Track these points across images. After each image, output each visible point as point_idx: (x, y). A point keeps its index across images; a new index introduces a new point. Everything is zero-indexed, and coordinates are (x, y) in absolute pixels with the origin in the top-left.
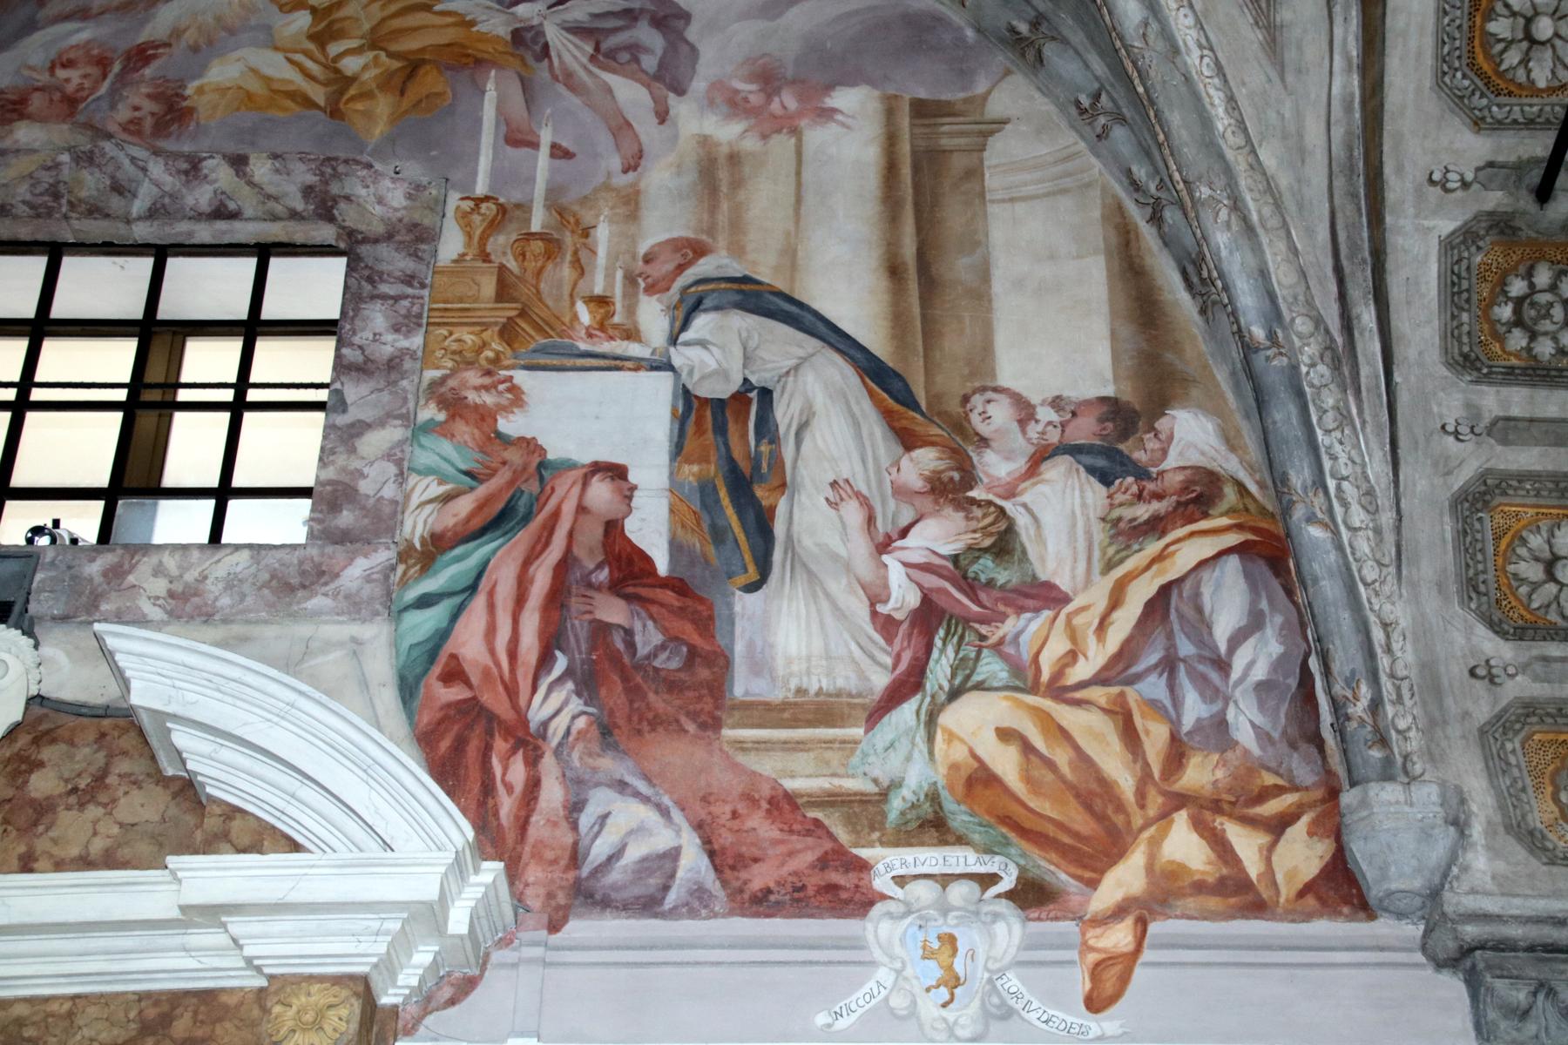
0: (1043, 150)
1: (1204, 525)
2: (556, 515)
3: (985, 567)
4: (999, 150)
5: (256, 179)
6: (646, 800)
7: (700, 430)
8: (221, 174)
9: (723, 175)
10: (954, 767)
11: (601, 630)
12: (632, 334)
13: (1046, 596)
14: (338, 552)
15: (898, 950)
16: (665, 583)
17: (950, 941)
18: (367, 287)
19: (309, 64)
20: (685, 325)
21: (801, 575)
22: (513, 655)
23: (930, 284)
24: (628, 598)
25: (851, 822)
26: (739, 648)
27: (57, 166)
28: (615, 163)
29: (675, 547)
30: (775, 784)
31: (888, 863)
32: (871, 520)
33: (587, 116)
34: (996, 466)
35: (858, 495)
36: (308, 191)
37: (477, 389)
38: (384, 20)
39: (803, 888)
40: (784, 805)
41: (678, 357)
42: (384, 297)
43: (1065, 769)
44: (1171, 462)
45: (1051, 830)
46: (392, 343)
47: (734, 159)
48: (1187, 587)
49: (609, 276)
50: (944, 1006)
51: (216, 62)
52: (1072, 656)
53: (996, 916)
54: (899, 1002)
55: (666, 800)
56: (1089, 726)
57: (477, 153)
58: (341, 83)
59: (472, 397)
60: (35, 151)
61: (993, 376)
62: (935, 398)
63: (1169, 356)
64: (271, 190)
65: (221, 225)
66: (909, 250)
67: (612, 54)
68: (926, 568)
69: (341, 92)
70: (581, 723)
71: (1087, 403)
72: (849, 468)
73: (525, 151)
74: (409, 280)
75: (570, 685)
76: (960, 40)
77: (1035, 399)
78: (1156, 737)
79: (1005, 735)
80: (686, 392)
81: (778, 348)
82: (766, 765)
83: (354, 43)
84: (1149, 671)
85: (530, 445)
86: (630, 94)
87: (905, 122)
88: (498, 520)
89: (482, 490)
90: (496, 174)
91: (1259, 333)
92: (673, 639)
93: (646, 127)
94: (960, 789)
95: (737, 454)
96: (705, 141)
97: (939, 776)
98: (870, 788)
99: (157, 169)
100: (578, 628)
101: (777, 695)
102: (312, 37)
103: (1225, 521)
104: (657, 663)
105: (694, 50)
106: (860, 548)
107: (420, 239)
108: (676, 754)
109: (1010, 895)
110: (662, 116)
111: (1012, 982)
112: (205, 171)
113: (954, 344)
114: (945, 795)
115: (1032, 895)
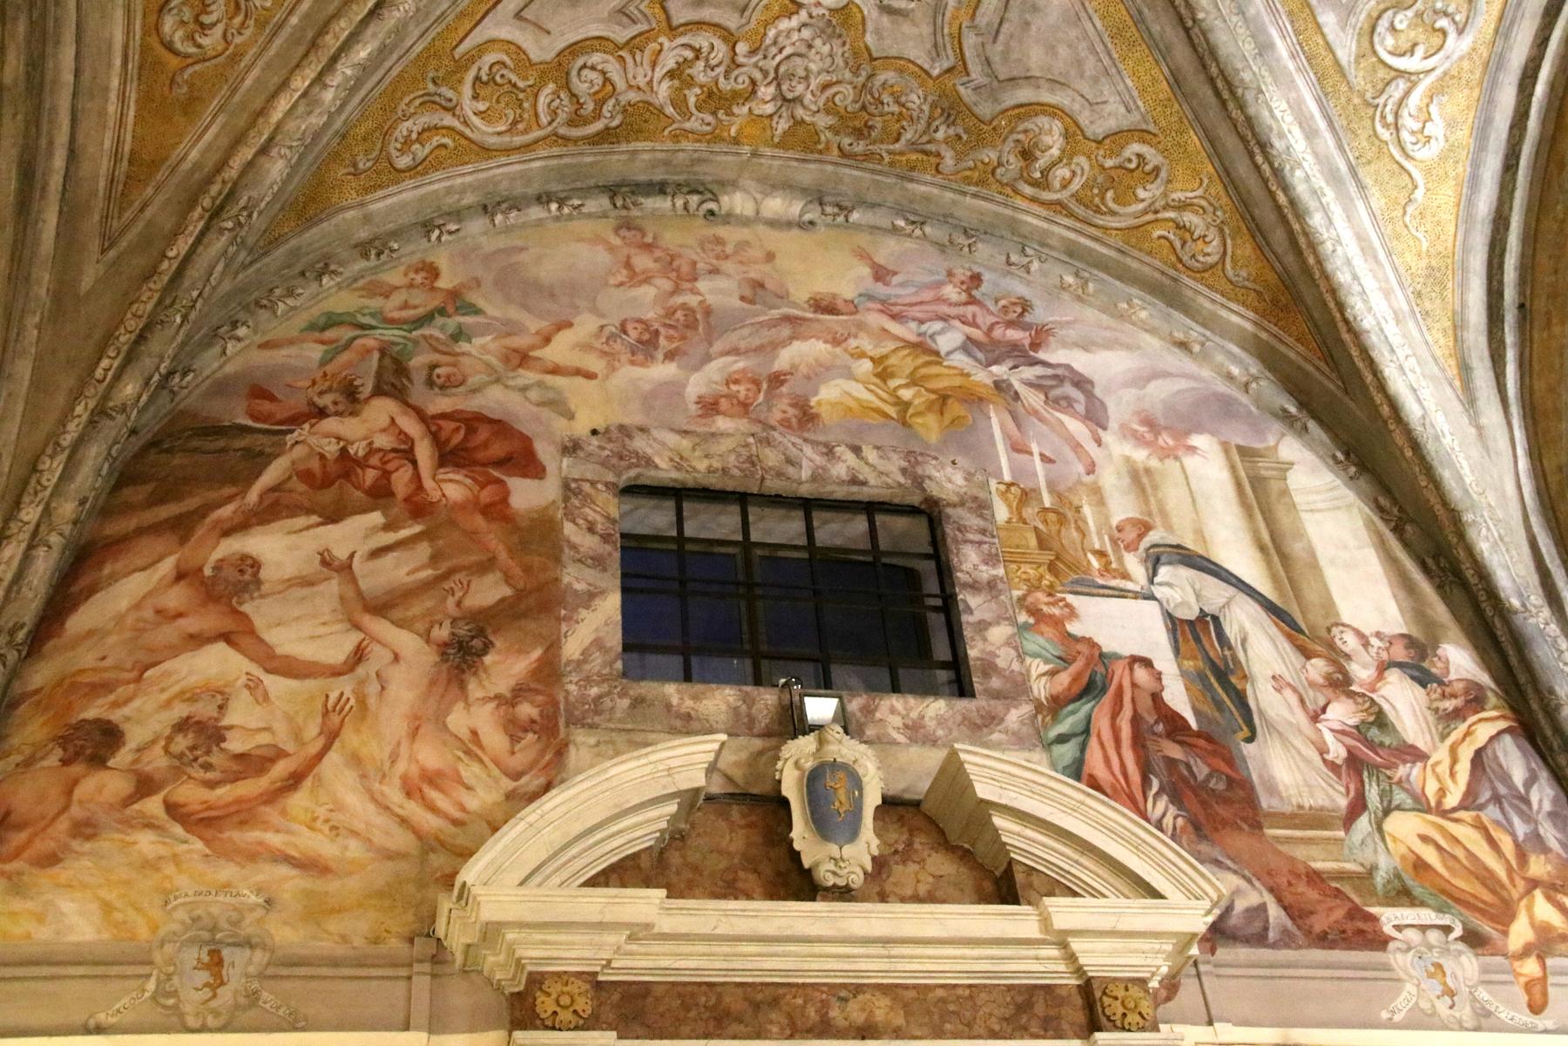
3: (1374, 733)
6: (1235, 872)
7: (1186, 641)
8: (850, 457)
9: (1145, 480)
10: (1403, 858)
11: (1171, 763)
13: (1415, 755)
15: (1412, 972)
16: (1199, 735)
17: (1438, 966)
18: (960, 535)
20: (1155, 573)
21: (1275, 735)
23: (1285, 558)
24: (1181, 743)
25: (1357, 889)
26: (1255, 778)
27: (747, 445)
28: (1081, 469)
29: (1197, 713)
31: (1389, 917)
32: (1302, 701)
34: (1361, 672)
35: (1289, 685)
37: (1048, 604)
38: (916, 368)
40: (1315, 878)
41: (1159, 592)
42: (972, 542)
43: (1465, 862)
45: (1472, 900)
47: (1148, 471)
48: (1489, 751)
49: (1101, 538)
50: (1451, 1007)
52: (1442, 792)
53: (1460, 953)
55: (1246, 872)
56: (1465, 833)
58: (904, 406)
60: (729, 435)
61: (1337, 614)
62: (1312, 628)
63: (1429, 612)
64: (881, 468)
65: (855, 489)
66: (1266, 537)
67: (1056, 401)
68: (1343, 733)
69: (905, 411)
74: (983, 532)
75: (1165, 797)
77: (1367, 632)
79: (1425, 839)
82: (1300, 853)
83: (903, 382)
86: (1075, 427)
87: (1237, 458)
88: (1090, 689)
90: (1012, 471)
93: (1090, 447)
94: (1410, 870)
95: (1212, 654)
96: (1127, 459)
97: (1397, 862)
98: (1360, 869)
99: (808, 450)
100: (1158, 764)
101: (1287, 809)
102: (878, 375)
103: (1494, 713)
104: (1211, 785)
105: (1102, 403)
106: (1301, 719)
108: (1240, 841)
110: (1099, 442)
111: (1483, 994)
114: (1404, 875)
115: (1473, 939)
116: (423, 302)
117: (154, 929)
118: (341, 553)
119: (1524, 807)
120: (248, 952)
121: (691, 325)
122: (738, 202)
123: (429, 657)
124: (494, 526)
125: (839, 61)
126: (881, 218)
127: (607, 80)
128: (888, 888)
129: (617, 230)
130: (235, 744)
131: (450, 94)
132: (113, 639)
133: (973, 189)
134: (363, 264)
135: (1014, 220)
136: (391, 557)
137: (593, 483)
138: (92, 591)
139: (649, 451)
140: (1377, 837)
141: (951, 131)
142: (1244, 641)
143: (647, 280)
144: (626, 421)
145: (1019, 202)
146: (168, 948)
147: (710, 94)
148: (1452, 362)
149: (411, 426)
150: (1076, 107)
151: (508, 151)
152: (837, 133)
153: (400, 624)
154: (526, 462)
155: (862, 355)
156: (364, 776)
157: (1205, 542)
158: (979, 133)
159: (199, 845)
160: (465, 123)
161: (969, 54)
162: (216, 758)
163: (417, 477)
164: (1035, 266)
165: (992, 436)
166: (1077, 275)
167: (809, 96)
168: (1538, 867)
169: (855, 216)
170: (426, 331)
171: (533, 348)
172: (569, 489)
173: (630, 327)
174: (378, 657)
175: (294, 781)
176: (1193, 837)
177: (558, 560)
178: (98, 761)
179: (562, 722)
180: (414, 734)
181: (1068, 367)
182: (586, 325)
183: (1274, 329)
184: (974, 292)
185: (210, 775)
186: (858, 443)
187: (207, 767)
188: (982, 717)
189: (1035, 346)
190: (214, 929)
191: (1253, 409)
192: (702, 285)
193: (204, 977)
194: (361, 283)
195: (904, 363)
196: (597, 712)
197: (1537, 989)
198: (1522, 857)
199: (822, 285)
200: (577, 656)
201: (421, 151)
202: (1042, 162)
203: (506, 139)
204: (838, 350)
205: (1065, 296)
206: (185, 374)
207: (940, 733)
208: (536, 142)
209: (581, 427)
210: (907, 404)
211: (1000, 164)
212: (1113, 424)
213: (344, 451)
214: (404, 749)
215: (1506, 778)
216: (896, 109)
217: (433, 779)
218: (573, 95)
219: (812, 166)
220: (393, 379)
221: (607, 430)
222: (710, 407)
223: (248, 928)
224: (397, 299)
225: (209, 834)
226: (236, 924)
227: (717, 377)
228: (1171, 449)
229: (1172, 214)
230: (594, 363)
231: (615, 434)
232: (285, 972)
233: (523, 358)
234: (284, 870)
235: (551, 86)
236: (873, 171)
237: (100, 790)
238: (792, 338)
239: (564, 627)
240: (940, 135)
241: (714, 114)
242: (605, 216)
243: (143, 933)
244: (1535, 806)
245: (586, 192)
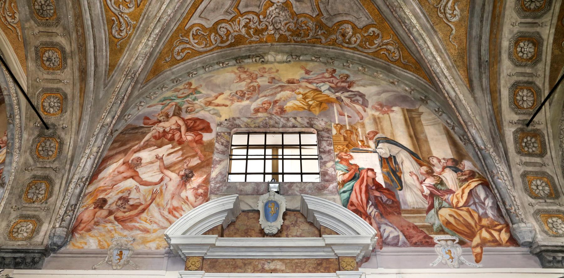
0: (430, 117)
1: (474, 180)
2: (363, 177)
3: (439, 187)
4: (423, 118)
6: (391, 227)
8: (293, 121)
9: (378, 120)
10: (443, 221)
11: (376, 197)
12: (369, 147)
13: (451, 192)
14: (327, 184)
16: (385, 189)
17: (450, 251)
20: (378, 145)
22: (362, 201)
23: (418, 139)
24: (380, 192)
25: (427, 230)
26: (401, 200)
27: (266, 120)
28: (359, 118)
29: (385, 183)
30: (413, 224)
31: (436, 238)
32: (418, 178)
33: (352, 111)
34: (437, 169)
36: (308, 123)
40: (415, 227)
41: (378, 150)
43: (462, 221)
44: (466, 169)
46: (328, 148)
47: (379, 118)
49: (362, 137)
52: (458, 202)
53: (457, 247)
54: (444, 262)
56: (464, 213)
58: (310, 106)
59: (344, 157)
61: (432, 154)
62: (423, 158)
65: (294, 129)
70: (377, 213)
71: (449, 159)
72: (412, 170)
73: (343, 116)
74: (328, 137)
76: (412, 100)
77: (440, 158)
78: (476, 216)
79: (450, 215)
80: (381, 157)
81: (395, 150)
82: (411, 221)
85: (356, 165)
86: (358, 107)
87: (406, 113)
88: (354, 178)
89: (350, 173)
90: (339, 120)
91: (483, 147)
92: (389, 199)
95: (392, 167)
96: (373, 115)
97: (441, 222)
99: (282, 120)
100: (372, 197)
101: (410, 209)
102: (303, 98)
106: (417, 183)
107: (329, 131)
108: (394, 218)
109: (458, 243)
110: (365, 111)
111: (462, 258)
113: (424, 149)
115: (462, 243)
116: (187, 92)
117: (109, 246)
118: (161, 155)
119: (483, 205)
120: (128, 251)
121: (254, 90)
122: (270, 58)
123: (179, 179)
124: (198, 145)
125: (288, 17)
126: (308, 57)
127: (228, 30)
128: (289, 233)
129: (237, 69)
130: (131, 203)
131: (187, 39)
132: (108, 179)
133: (331, 47)
134: (173, 84)
135: (344, 54)
136: (172, 155)
137: (224, 133)
138: (105, 168)
139: (240, 123)
140: (436, 216)
141: (322, 32)
142: (402, 163)
143: (244, 80)
144: (234, 116)
146: (111, 250)
147: (256, 30)
149: (181, 123)
150: (354, 20)
151: (206, 52)
152: (292, 36)
153: (172, 171)
154: (208, 129)
155: (300, 93)
156: (159, 209)
157: (394, 136)
158: (329, 31)
159: (120, 226)
160: (193, 46)
161: (322, 10)
162: (127, 206)
163: (181, 135)
164: (351, 65)
165: (334, 112)
166: (362, 67)
167: (282, 27)
168: (485, 222)
169: (301, 58)
170: (187, 99)
171: (213, 100)
172: (218, 135)
173: (238, 93)
174: (166, 179)
175: (143, 210)
176: (380, 217)
177: (213, 153)
178: (101, 208)
179: (209, 193)
180: (172, 198)
181: (358, 92)
182: (227, 93)
183: (417, 76)
184: (334, 75)
185: (125, 210)
187: (124, 208)
189: (349, 87)
190: (122, 246)
192: (258, 80)
193: (118, 257)
194: (173, 89)
195: (311, 95)
196: (218, 191)
197: (479, 256)
198: (480, 219)
199: (290, 77)
200: (215, 177)
201: (183, 55)
202: (348, 37)
203: (205, 49)
204: (293, 93)
205: (360, 73)
206: (128, 116)
208: (213, 49)
209: (223, 119)
210: (311, 105)
211: (337, 39)
212: (370, 106)
213: (164, 130)
214: (169, 202)
215: (478, 197)
216: (306, 28)
217: (175, 209)
218: (220, 35)
220: (178, 112)
221: (229, 119)
222: (257, 111)
223: (129, 246)
224: (181, 92)
225: (123, 224)
226: (126, 245)
227: (260, 103)
229: (384, 47)
230: (228, 103)
231: (231, 120)
232: (136, 256)
233: (210, 103)
234: (138, 232)
235: (213, 34)
237: (101, 214)
238: (281, 91)
239: (212, 169)
240: (319, 33)
241: (258, 35)
242: (235, 65)
243: (106, 247)
244: (486, 205)
245: (229, 60)
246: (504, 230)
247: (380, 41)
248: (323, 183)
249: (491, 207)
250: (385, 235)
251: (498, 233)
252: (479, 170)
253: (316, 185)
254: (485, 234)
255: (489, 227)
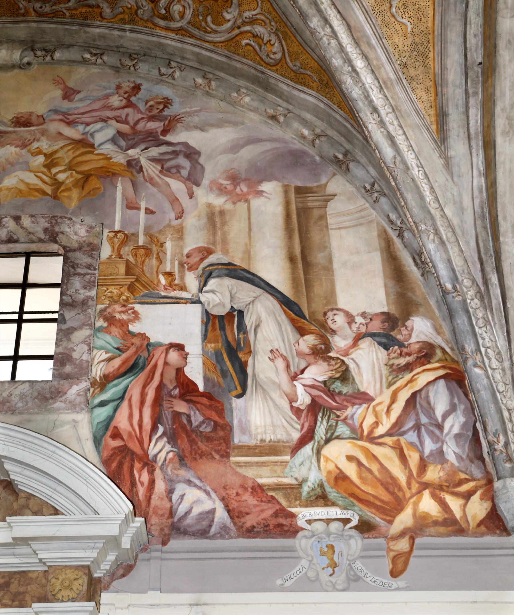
1: (428, 366)
2: (155, 366)
3: (337, 386)
4: (333, 207)
5: (25, 225)
6: (200, 488)
7: (214, 329)
9: (218, 220)
11: (177, 415)
12: (183, 288)
13: (364, 398)
14: (65, 383)
15: (310, 552)
16: (203, 395)
17: (331, 547)
18: (72, 270)
19: (44, 177)
20: (205, 284)
21: (260, 391)
22: (140, 426)
23: (307, 265)
24: (188, 401)
25: (287, 497)
26: (235, 422)
28: (172, 215)
29: (206, 379)
30: (254, 481)
31: (304, 514)
32: (288, 366)
33: (160, 196)
35: (282, 355)
36: (46, 230)
37: (120, 312)
38: (74, 158)
39: (268, 525)
40: (258, 490)
41: (203, 297)
42: (79, 274)
43: (376, 473)
44: (413, 340)
45: (372, 499)
46: (83, 294)
47: (222, 213)
48: (423, 393)
49: (172, 264)
50: (331, 576)
51: (6, 177)
52: (376, 424)
53: (351, 537)
54: (311, 574)
55: (208, 488)
56: (385, 454)
57: (115, 213)
58: (57, 184)
59: (118, 316)
61: (336, 303)
62: (312, 314)
63: (410, 294)
64: (30, 230)
65: (11, 245)
66: (297, 250)
67: (169, 170)
68: (312, 387)
69: (58, 189)
70: (171, 455)
71: (376, 315)
72: (278, 344)
73: (135, 211)
74: (89, 267)
75: (165, 439)
77: (354, 313)
78: (414, 458)
79: (350, 458)
80: (207, 313)
81: (245, 292)
82: (250, 473)
83: (62, 168)
84: (409, 430)
85: (143, 336)
86: (177, 186)
87: (292, 196)
88: (131, 369)
89: (124, 356)
91: (449, 286)
92: (207, 419)
93: (185, 200)
94: (332, 482)
95: (230, 338)
97: (323, 476)
98: (294, 482)
100: (167, 415)
101: (253, 442)
102: (45, 166)
103: (437, 365)
104: (201, 429)
105: (203, 167)
106: (284, 379)
107: (93, 250)
108: (211, 468)
109: (356, 528)
110: (191, 195)
111: (359, 565)
112: (4, 223)
113: (319, 290)
114: (326, 484)
115: (365, 527)
119: (437, 432)
126: (74, 54)
133: (128, 27)
135: (160, 44)
140: (314, 458)
142: (257, 327)
145: (158, 31)
148: (432, 112)
155: (39, 152)
157: (249, 258)
164: (177, 74)
165: (115, 199)
166: (204, 77)
168: (433, 474)
169: (57, 55)
176: (177, 466)
181: (185, 144)
183: (326, 100)
184: (133, 99)
186: (19, 213)
188: (51, 392)
189: (165, 132)
191: (317, 158)
195: (66, 156)
198: (423, 466)
199: (24, 107)
205: (199, 93)
207: (20, 405)
210: (62, 183)
211: (138, 8)
212: (205, 182)
215: (430, 410)
219: (22, 25)
228: (245, 195)
229: (248, 28)
236: (62, 23)
244: (446, 431)
246: (479, 493)
247: (236, 14)
248: (55, 383)
249: (457, 436)
250: (182, 510)
251: (461, 502)
252: (447, 342)
253: (37, 387)
254: (428, 505)
255: (441, 488)
